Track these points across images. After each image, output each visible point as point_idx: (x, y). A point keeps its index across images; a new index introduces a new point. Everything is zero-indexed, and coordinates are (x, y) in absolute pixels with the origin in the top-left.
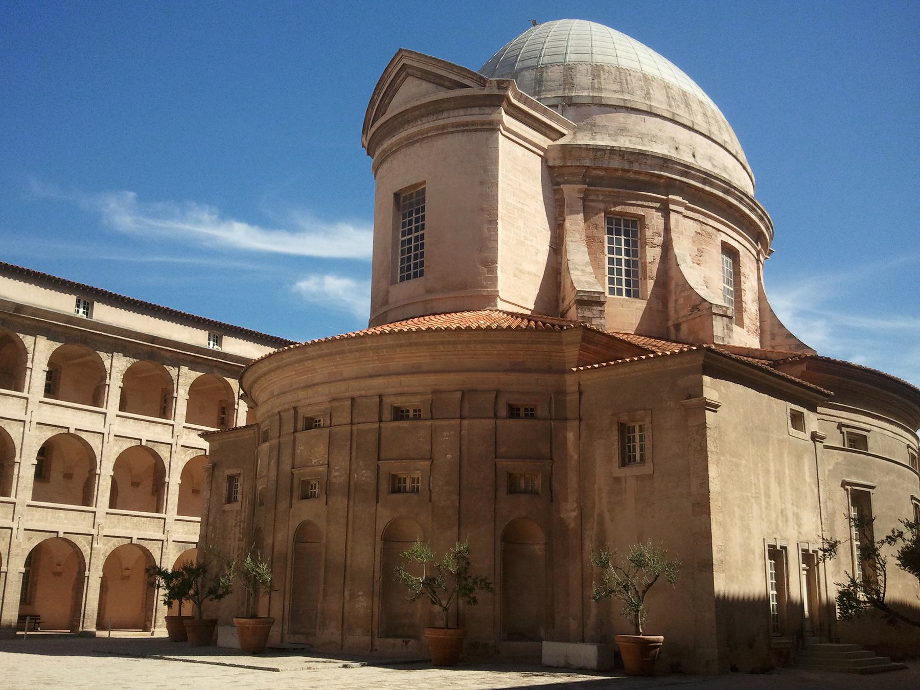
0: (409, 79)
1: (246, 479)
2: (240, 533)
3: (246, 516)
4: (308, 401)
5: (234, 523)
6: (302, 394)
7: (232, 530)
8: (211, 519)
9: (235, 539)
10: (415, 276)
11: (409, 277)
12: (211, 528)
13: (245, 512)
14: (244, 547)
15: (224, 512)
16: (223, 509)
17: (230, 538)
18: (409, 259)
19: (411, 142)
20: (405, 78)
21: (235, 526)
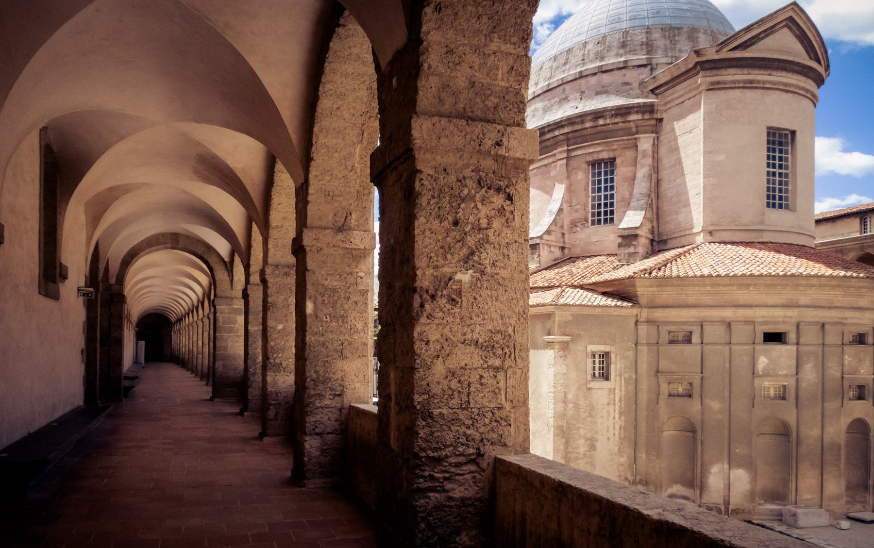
0: (786, 30)
1: (618, 358)
2: (614, 410)
3: (623, 395)
4: (855, 321)
5: (606, 401)
6: (848, 314)
7: (604, 408)
8: (570, 397)
9: (609, 416)
10: (780, 206)
11: (774, 206)
12: (571, 405)
13: (620, 390)
14: (622, 426)
15: (589, 389)
16: (588, 386)
17: (602, 416)
18: (774, 190)
19: (786, 89)
20: (783, 27)
21: (608, 404)
